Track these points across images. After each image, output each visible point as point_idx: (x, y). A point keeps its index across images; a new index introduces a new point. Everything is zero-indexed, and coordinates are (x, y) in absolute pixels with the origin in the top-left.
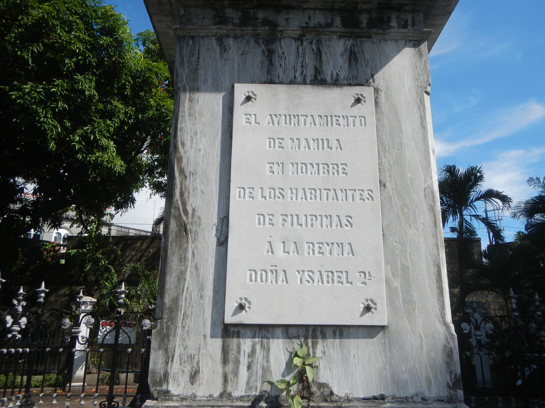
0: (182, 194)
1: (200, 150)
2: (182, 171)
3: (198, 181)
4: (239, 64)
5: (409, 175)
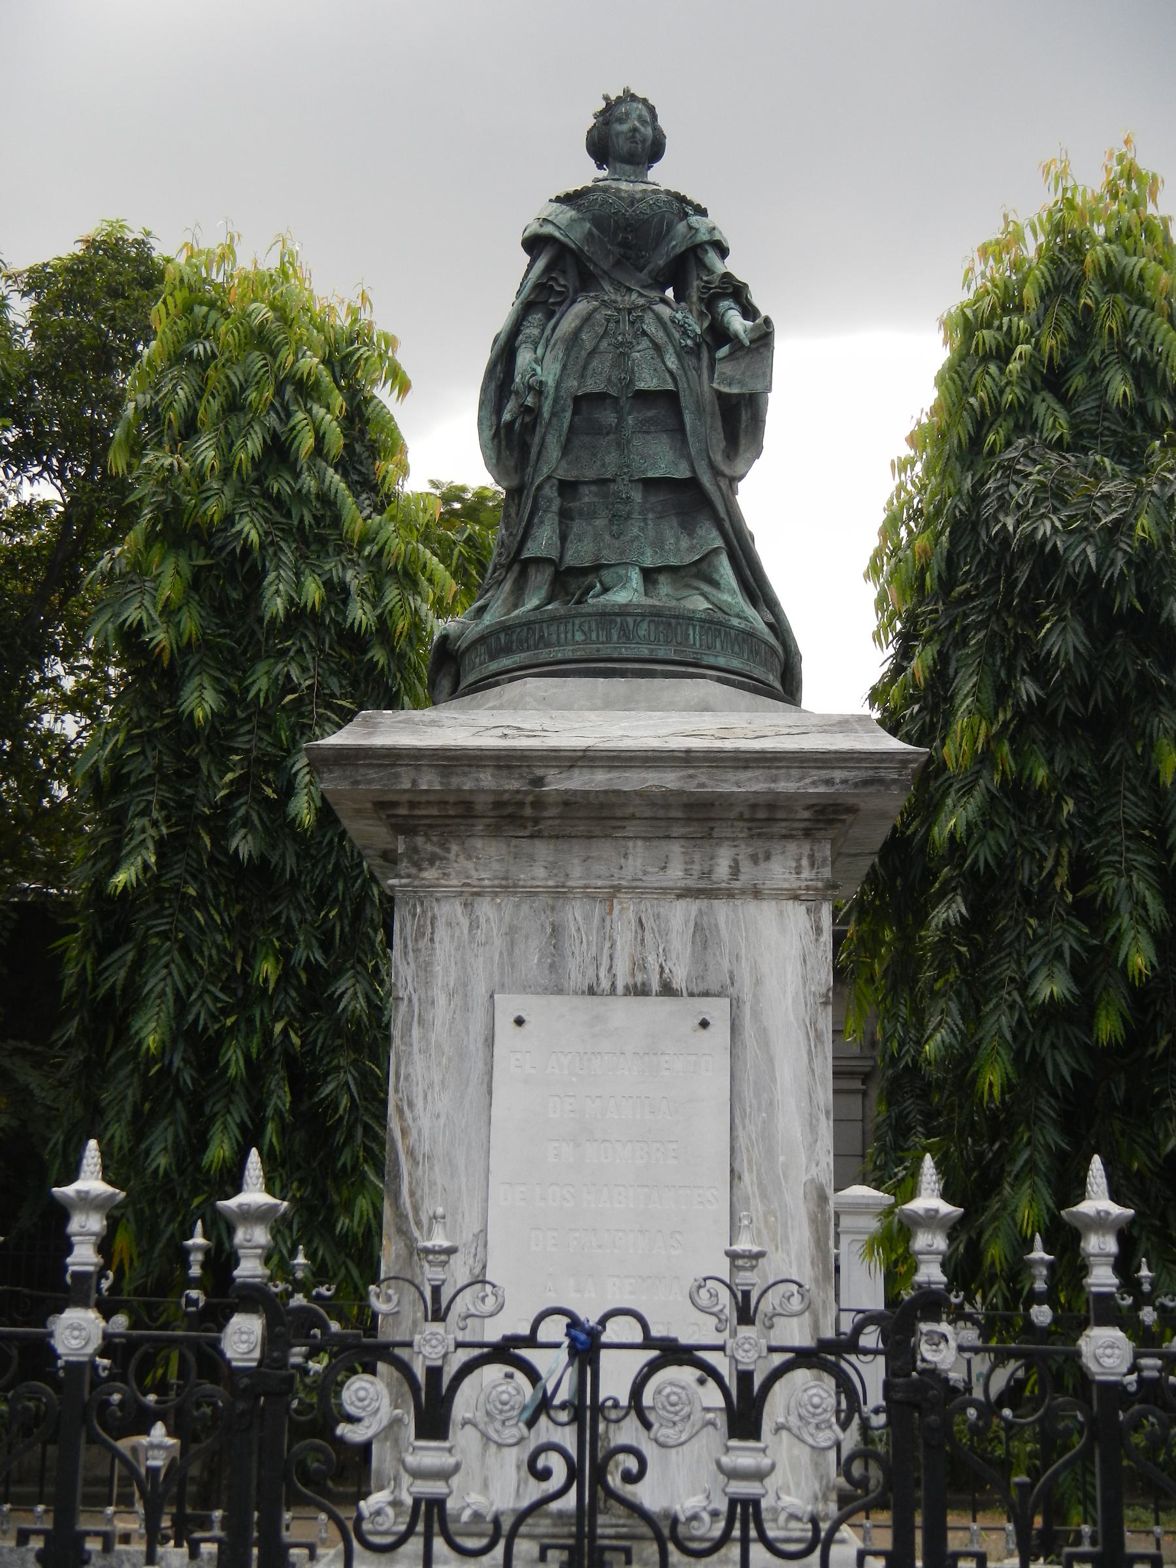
0: (412, 1194)
1: (438, 1116)
2: (411, 1153)
3: (437, 1169)
4: (501, 953)
5: (782, 1159)
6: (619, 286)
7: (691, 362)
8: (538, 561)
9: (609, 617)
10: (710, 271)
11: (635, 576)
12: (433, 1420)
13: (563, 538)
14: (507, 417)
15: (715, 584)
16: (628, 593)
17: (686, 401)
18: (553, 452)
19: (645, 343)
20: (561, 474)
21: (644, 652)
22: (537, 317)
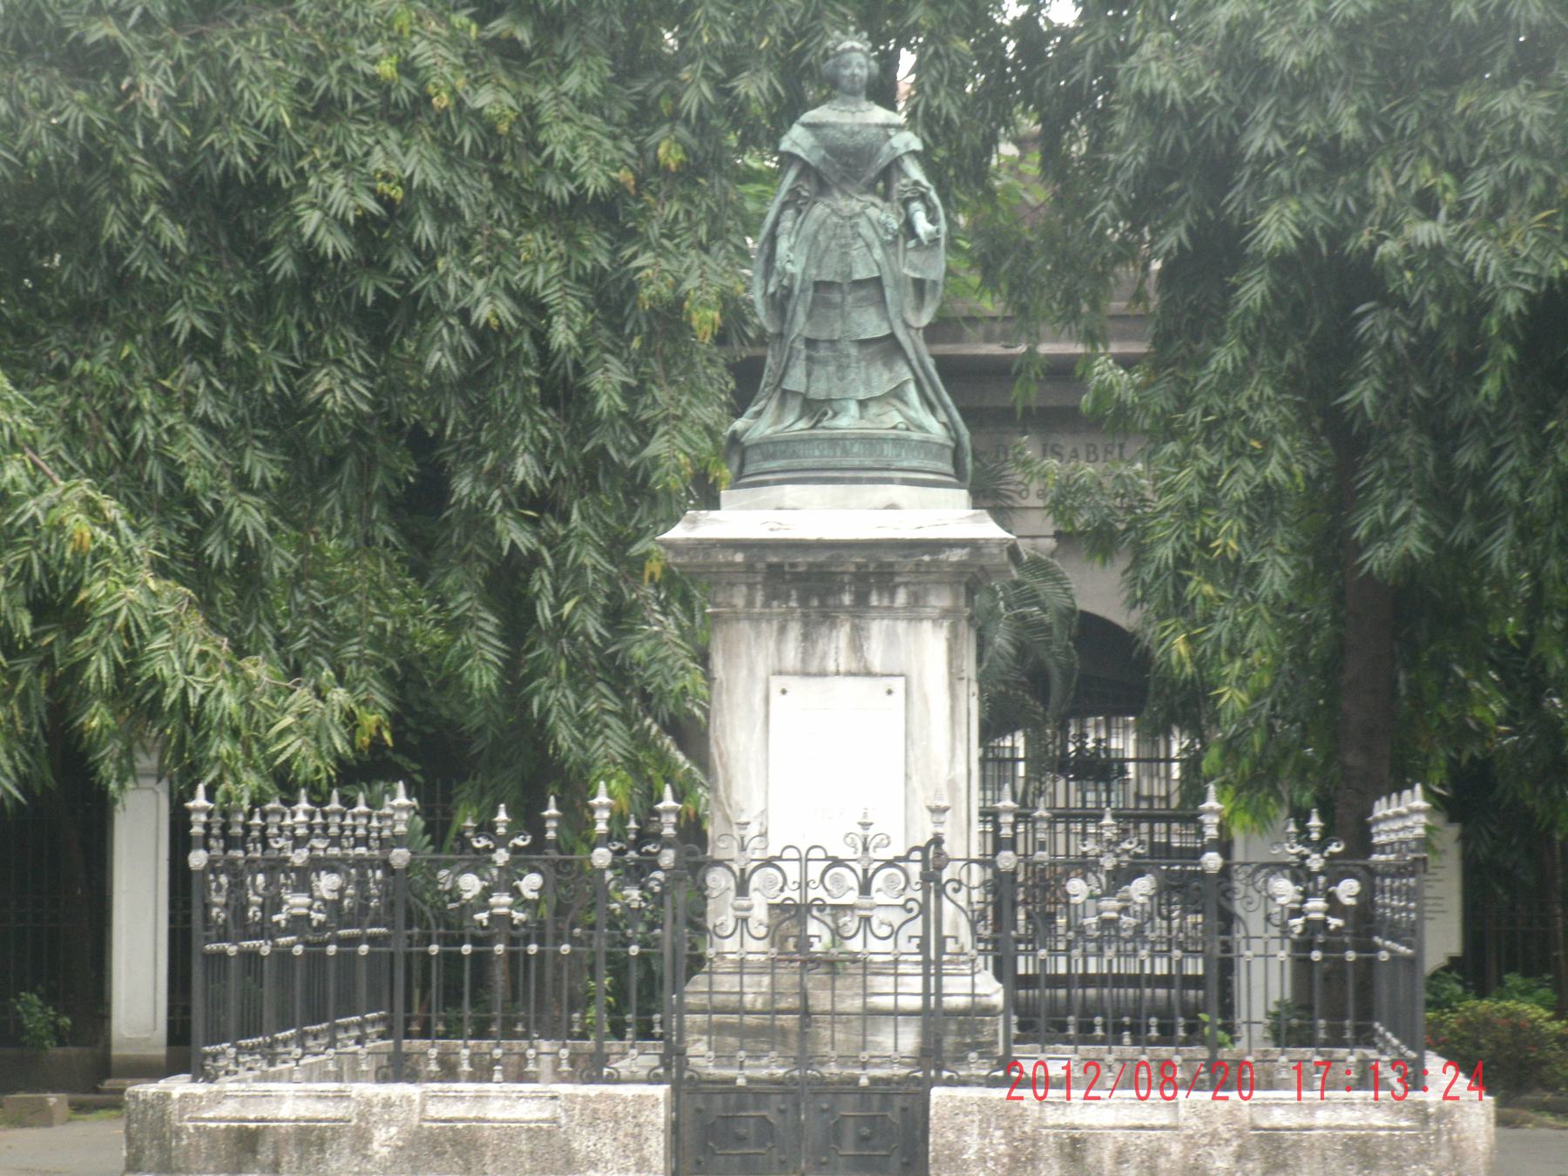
6: (844, 193)
7: (890, 250)
8: (794, 394)
9: (837, 441)
10: (906, 176)
11: (853, 408)
12: (742, 888)
13: (809, 375)
14: (771, 289)
15: (906, 403)
16: (848, 421)
17: (888, 281)
18: (801, 318)
19: (860, 243)
20: (806, 333)
21: (856, 462)
22: (790, 212)
